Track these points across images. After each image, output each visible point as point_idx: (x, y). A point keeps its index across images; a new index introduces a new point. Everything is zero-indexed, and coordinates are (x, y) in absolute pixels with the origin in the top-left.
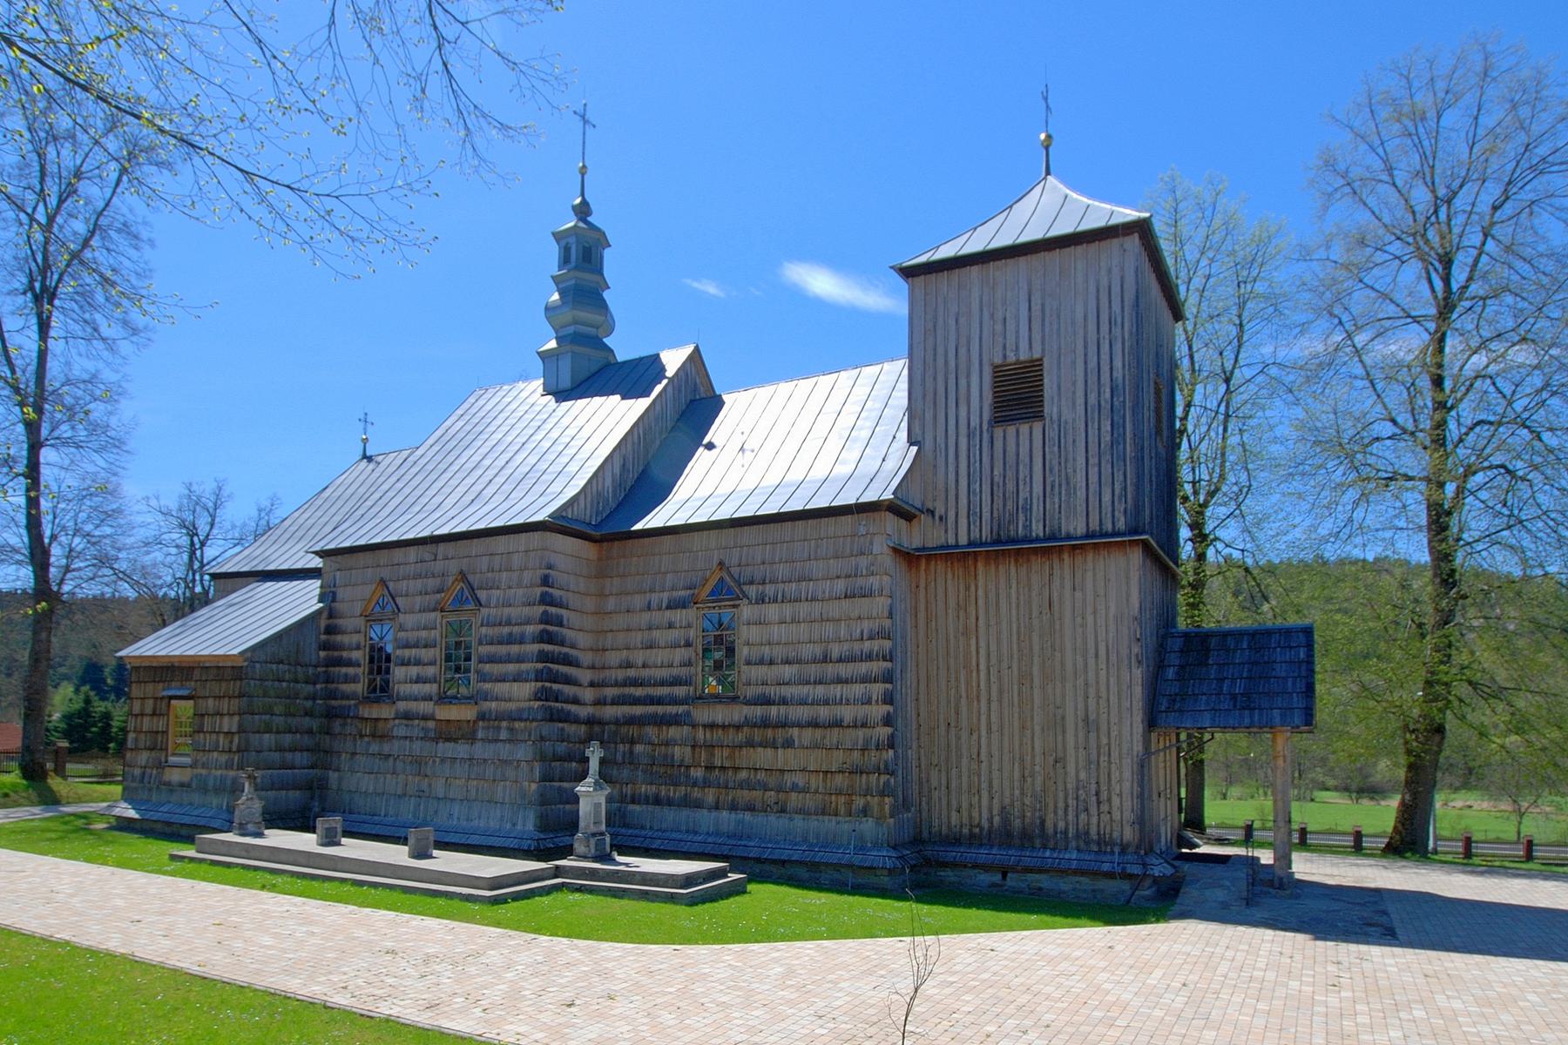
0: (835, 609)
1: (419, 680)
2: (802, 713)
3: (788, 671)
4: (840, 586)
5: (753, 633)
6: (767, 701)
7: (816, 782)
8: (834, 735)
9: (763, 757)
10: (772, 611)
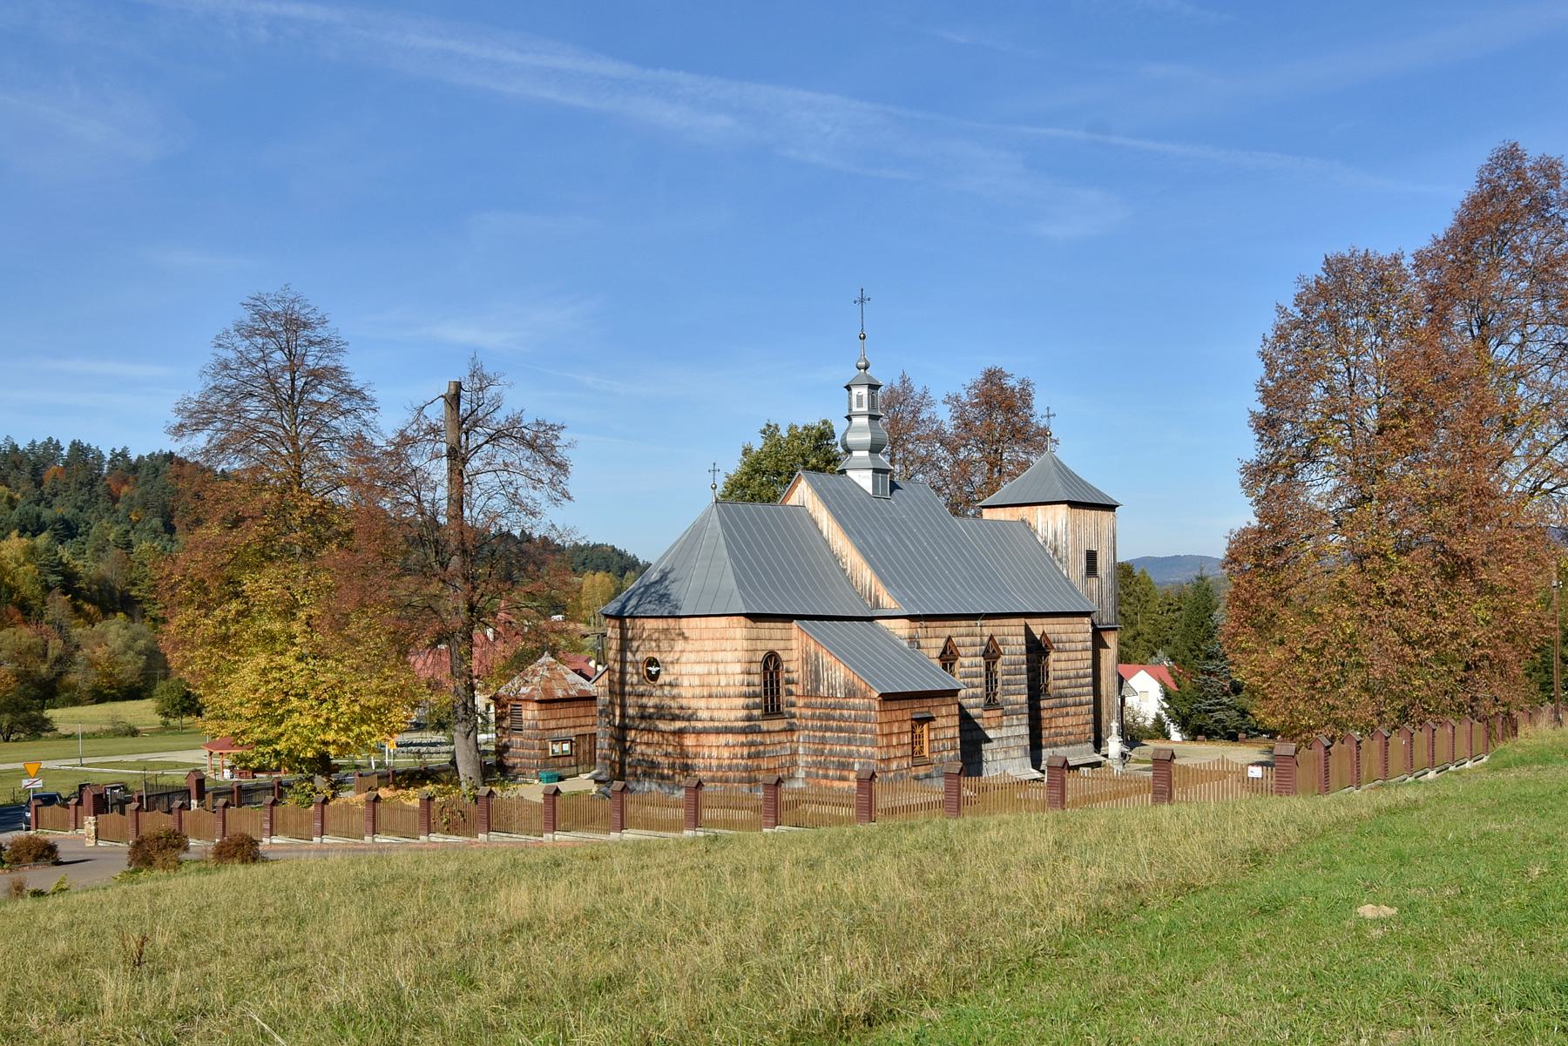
0: (1079, 655)
1: (974, 696)
2: (1070, 700)
3: (1065, 682)
4: (1080, 646)
5: (1058, 665)
6: (1061, 696)
7: (1076, 730)
8: (1080, 709)
9: (1060, 721)
10: (1064, 656)
